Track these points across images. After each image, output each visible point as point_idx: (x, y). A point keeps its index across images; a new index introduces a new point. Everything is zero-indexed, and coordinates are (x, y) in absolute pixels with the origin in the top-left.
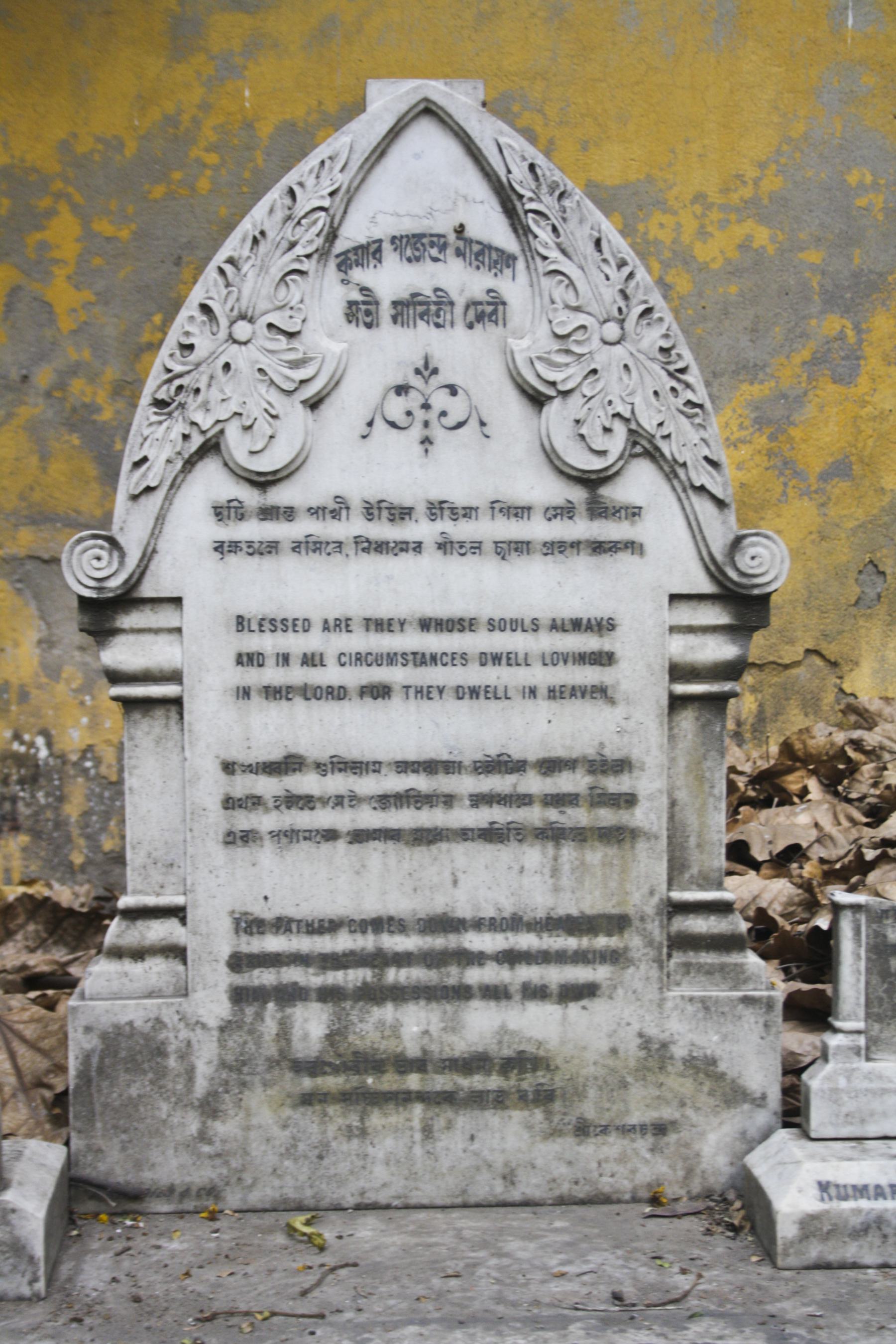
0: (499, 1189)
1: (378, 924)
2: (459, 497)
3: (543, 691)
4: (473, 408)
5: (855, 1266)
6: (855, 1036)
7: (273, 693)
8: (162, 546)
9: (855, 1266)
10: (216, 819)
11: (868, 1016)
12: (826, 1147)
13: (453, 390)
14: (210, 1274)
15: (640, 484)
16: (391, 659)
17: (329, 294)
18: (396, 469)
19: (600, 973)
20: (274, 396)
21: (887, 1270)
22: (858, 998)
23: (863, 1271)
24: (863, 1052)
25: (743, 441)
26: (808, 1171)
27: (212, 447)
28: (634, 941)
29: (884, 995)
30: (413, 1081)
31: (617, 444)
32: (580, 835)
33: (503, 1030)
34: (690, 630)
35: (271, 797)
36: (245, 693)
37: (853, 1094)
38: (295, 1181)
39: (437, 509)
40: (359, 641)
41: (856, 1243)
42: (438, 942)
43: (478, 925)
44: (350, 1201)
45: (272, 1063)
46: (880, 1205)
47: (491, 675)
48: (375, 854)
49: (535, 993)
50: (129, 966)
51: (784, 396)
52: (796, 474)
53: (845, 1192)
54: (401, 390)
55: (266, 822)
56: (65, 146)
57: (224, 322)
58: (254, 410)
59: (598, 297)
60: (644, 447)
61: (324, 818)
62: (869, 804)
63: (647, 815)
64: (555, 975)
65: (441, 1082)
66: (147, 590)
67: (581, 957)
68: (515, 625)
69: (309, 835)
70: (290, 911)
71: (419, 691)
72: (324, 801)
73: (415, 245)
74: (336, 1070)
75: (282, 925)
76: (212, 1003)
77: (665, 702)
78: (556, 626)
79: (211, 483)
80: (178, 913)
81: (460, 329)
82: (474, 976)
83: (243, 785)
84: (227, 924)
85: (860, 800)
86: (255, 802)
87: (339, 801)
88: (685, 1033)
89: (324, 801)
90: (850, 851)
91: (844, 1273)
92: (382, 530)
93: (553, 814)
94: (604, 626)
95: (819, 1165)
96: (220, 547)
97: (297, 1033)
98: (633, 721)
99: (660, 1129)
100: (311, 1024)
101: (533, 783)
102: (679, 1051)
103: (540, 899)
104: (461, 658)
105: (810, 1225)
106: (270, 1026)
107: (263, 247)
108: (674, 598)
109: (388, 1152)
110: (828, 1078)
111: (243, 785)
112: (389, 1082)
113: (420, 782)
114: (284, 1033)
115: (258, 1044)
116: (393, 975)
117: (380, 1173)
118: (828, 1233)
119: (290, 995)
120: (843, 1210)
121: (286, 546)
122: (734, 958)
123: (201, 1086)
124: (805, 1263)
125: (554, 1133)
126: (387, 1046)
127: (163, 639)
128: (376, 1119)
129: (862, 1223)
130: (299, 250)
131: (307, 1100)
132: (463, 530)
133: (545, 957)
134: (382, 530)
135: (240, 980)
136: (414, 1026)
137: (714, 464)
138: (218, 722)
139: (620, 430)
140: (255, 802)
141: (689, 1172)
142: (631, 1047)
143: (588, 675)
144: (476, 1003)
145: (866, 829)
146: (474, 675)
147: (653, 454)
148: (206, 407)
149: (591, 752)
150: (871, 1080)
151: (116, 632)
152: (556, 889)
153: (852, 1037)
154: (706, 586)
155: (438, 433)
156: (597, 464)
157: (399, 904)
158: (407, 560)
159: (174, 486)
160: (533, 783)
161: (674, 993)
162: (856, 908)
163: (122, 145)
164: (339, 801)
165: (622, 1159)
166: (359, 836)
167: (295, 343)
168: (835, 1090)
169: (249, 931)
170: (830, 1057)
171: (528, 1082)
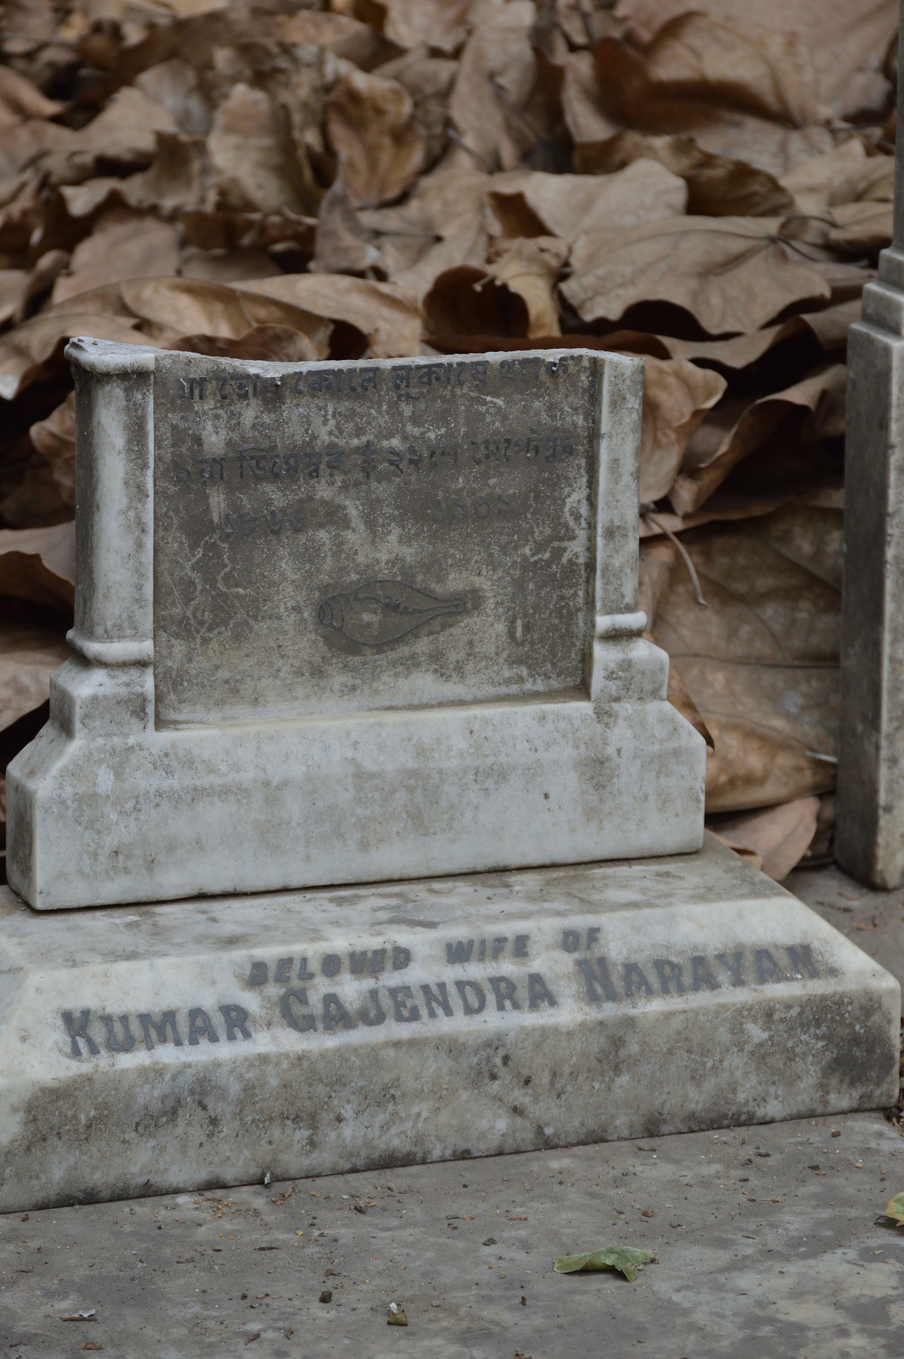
5: (148, 1191)
6: (134, 673)
9: (148, 1191)
11: (159, 624)
12: (70, 929)
21: (219, 1193)
22: (139, 588)
23: (167, 1200)
24: (150, 709)
26: (38, 990)
29: (197, 577)
37: (130, 805)
41: (152, 1142)
46: (201, 1054)
53: (123, 1032)
62: (51, 65)
85: (30, 56)
90: (22, 187)
91: (124, 1207)
95: (63, 974)
110: (73, 772)
118: (89, 1126)
120: (123, 1072)
124: (39, 1196)
129: (164, 1098)
145: (54, 131)
150: (169, 772)
153: (123, 677)
162: (134, 377)
168: (90, 799)
170: (77, 725)
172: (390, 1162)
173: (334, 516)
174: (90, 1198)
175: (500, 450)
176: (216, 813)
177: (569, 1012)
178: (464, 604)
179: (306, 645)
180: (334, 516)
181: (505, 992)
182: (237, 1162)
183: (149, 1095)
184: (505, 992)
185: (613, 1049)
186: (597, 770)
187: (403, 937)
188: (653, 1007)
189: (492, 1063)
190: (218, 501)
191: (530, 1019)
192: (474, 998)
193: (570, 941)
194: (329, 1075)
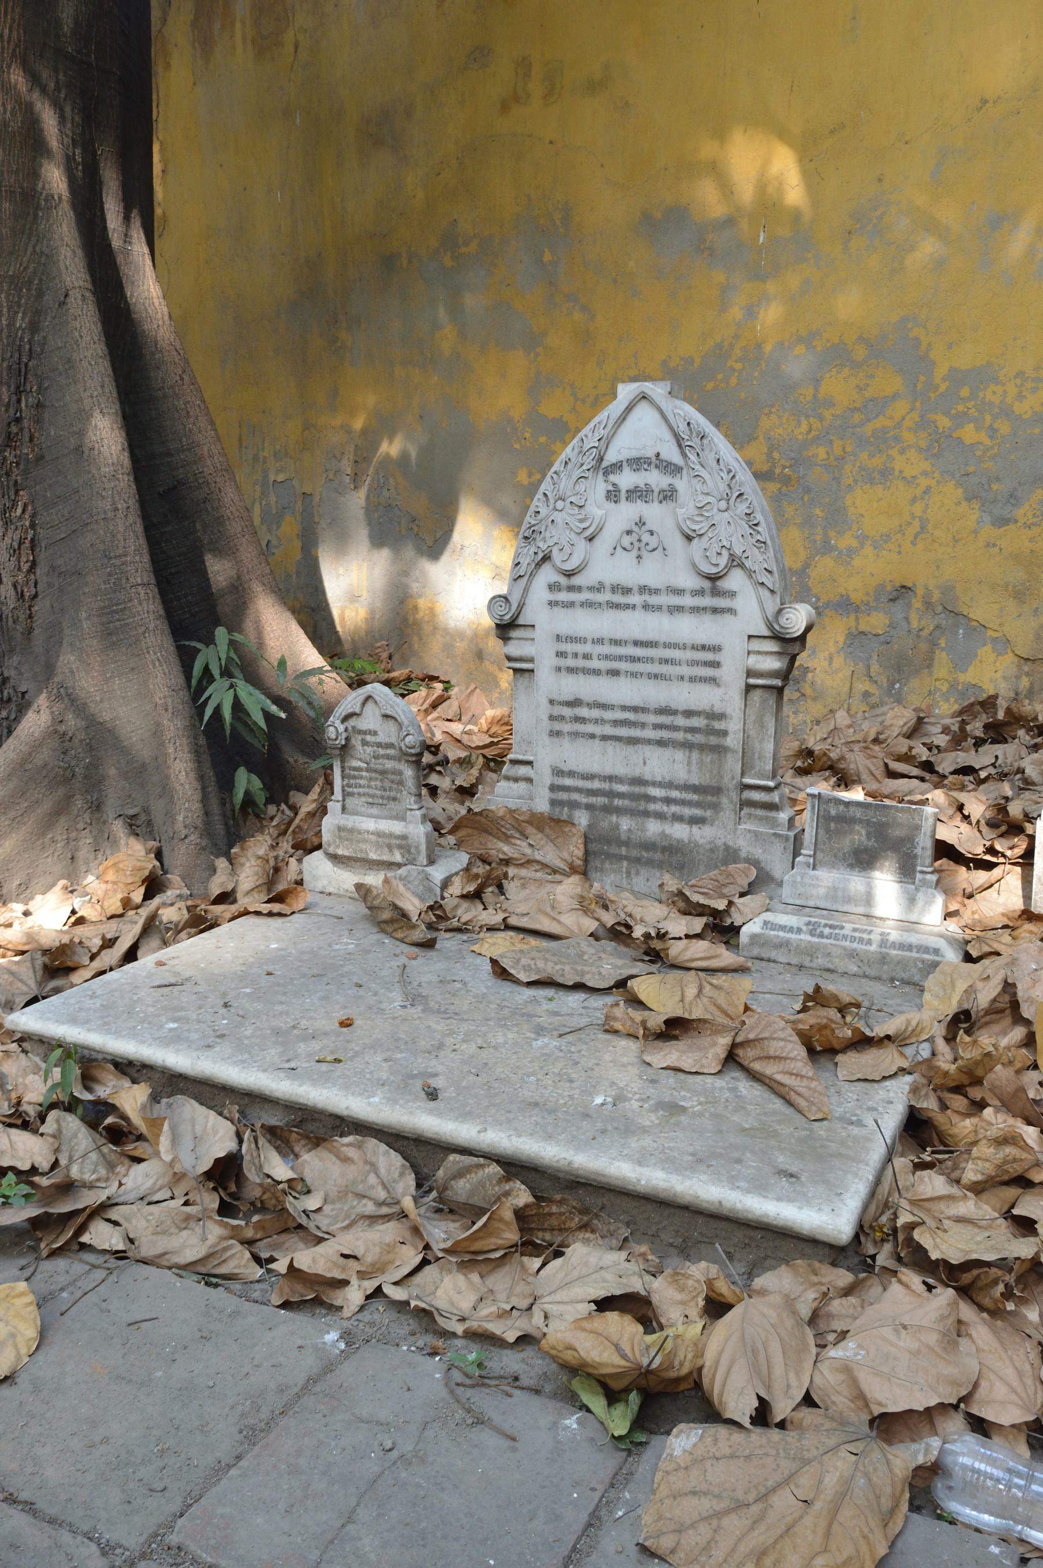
1: (611, 778)
2: (653, 584)
3: (687, 678)
4: (660, 542)
7: (571, 670)
9: (774, 961)
10: (546, 725)
13: (652, 533)
15: (735, 581)
16: (620, 658)
17: (601, 487)
18: (622, 569)
19: (708, 813)
20: (573, 535)
27: (546, 558)
30: (623, 851)
31: (723, 561)
33: (663, 832)
34: (759, 653)
35: (569, 717)
36: (559, 669)
39: (643, 589)
40: (606, 649)
42: (637, 790)
43: (654, 784)
47: (664, 669)
48: (610, 746)
49: (678, 818)
50: (512, 784)
54: (629, 532)
55: (567, 728)
57: (552, 501)
59: (718, 490)
60: (735, 562)
61: (590, 728)
63: (732, 741)
64: (687, 811)
65: (634, 853)
66: (521, 621)
67: (698, 805)
68: (675, 646)
70: (574, 768)
71: (632, 674)
73: (638, 463)
75: (571, 774)
78: (694, 647)
79: (547, 575)
80: (529, 763)
81: (656, 504)
82: (652, 807)
83: (558, 710)
84: (549, 771)
87: (596, 721)
88: (744, 845)
89: (590, 721)
93: (689, 736)
94: (716, 649)
96: (552, 604)
98: (726, 697)
101: (680, 721)
102: (743, 854)
104: (650, 660)
105: (754, 938)
107: (570, 466)
108: (750, 637)
111: (558, 710)
113: (630, 716)
116: (617, 802)
121: (578, 604)
122: (773, 814)
130: (585, 467)
132: (654, 600)
133: (683, 803)
135: (554, 796)
138: (549, 682)
139: (725, 553)
140: (562, 718)
146: (656, 668)
147: (742, 566)
148: (544, 540)
149: (707, 708)
151: (509, 639)
152: (689, 772)
154: (766, 633)
155: (645, 554)
156: (714, 570)
157: (620, 770)
158: (629, 612)
159: (532, 575)
160: (680, 721)
161: (742, 827)
164: (596, 721)
166: (604, 738)
167: (582, 511)
168: (794, 882)
169: (558, 775)
174: (762, 959)
182: (795, 961)
190: (833, 825)
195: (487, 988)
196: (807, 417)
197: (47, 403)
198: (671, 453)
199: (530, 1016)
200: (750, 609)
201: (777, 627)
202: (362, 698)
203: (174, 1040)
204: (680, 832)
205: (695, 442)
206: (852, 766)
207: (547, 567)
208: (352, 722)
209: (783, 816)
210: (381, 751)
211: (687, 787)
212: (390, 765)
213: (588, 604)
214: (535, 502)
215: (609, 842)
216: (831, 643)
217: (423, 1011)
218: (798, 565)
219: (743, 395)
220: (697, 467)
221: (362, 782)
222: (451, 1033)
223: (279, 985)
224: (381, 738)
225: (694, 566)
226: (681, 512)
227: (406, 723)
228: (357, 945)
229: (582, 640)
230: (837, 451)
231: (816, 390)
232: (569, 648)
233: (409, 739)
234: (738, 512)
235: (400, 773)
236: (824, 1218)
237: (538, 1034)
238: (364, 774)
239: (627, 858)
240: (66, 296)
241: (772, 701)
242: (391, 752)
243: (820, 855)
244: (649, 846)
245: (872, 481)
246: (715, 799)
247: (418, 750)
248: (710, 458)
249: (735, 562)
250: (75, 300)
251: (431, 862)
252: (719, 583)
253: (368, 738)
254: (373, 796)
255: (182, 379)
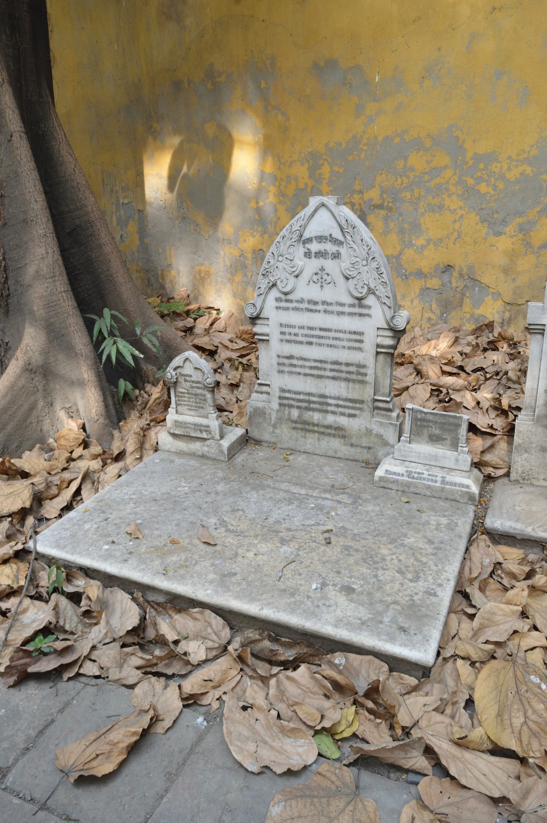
0: (333, 454)
1: (309, 394)
2: (329, 300)
3: (346, 347)
4: (332, 279)
7: (288, 341)
8: (265, 306)
13: (328, 275)
14: (261, 463)
15: (371, 300)
16: (313, 336)
17: (301, 250)
18: (313, 292)
19: (357, 412)
20: (287, 275)
25: (515, 236)
28: (365, 406)
30: (316, 428)
31: (365, 291)
32: (354, 381)
33: (335, 421)
34: (383, 336)
35: (287, 364)
36: (282, 340)
38: (291, 444)
39: (324, 303)
40: (306, 332)
42: (322, 400)
43: (330, 398)
44: (302, 450)
45: (287, 420)
47: (335, 342)
48: (309, 379)
49: (343, 414)
51: (530, 222)
52: (531, 247)
54: (316, 274)
55: (286, 369)
56: (326, 145)
57: (276, 257)
58: (283, 278)
60: (371, 291)
61: (298, 370)
63: (370, 378)
64: (347, 411)
65: (322, 430)
66: (262, 316)
67: (353, 408)
68: (341, 331)
69: (295, 373)
70: (291, 389)
72: (298, 366)
73: (320, 239)
74: (300, 423)
75: (289, 391)
76: (275, 405)
77: (375, 353)
78: (350, 333)
80: (268, 385)
81: (330, 260)
82: (329, 408)
84: (278, 390)
86: (284, 364)
87: (301, 367)
88: (376, 429)
89: (298, 366)
92: (311, 307)
93: (348, 376)
94: (361, 334)
96: (277, 308)
97: (292, 414)
98: (367, 356)
99: (369, 448)
100: (295, 413)
101: (344, 368)
102: (374, 432)
103: (344, 393)
106: (287, 412)
107: (285, 239)
108: (378, 328)
109: (310, 442)
112: (311, 428)
114: (289, 414)
115: (284, 415)
116: (312, 405)
117: (309, 446)
119: (291, 406)
122: (389, 413)
123: (273, 422)
125: (346, 445)
126: (310, 420)
127: (266, 326)
128: (308, 435)
131: (294, 428)
132: (329, 308)
133: (345, 407)
134: (311, 307)
135: (281, 402)
136: (316, 417)
137: (388, 297)
139: (366, 287)
140: (284, 364)
141: (375, 459)
142: (363, 429)
143: (357, 345)
144: (329, 414)
146: (331, 342)
147: (374, 293)
148: (273, 276)
149: (357, 362)
151: (256, 324)
152: (348, 392)
154: (386, 327)
155: (324, 285)
156: (360, 295)
157: (313, 390)
158: (317, 314)
159: (267, 293)
160: (344, 368)
163: (341, 144)
164: (301, 367)
165: (360, 453)
166: (305, 375)
171: (341, 433)
172: (417, 494)
173: (431, 427)
175: (451, 424)
176: (413, 454)
177: (438, 485)
178: (445, 439)
179: (427, 439)
180: (431, 427)
181: (432, 480)
183: (392, 480)
184: (432, 480)
185: (443, 490)
186: (457, 460)
187: (424, 472)
188: (448, 487)
189: (428, 487)
190: (419, 423)
191: (433, 484)
192: (428, 480)
193: (442, 477)
194: (411, 483)
195: (255, 514)
196: (401, 176)
197: (6, 195)
198: (337, 234)
199: (278, 532)
200: (378, 315)
201: (392, 325)
202: (184, 359)
203: (108, 556)
204: (343, 421)
205: (350, 230)
206: (424, 368)
207: (274, 290)
208: (179, 370)
209: (394, 414)
210: (195, 385)
211: (346, 400)
212: (199, 391)
213: (296, 309)
214: (267, 257)
215: (309, 424)
216: (413, 293)
217: (226, 531)
218: (396, 254)
219: (368, 164)
220: (351, 243)
221: (185, 399)
222: (241, 546)
223: (154, 517)
224: (194, 378)
225: (350, 292)
226: (343, 265)
227: (206, 372)
228: (189, 487)
229: (293, 327)
230: (416, 194)
231: (406, 162)
232: (287, 330)
233: (208, 380)
234: (372, 266)
235: (205, 396)
236: (422, 655)
237: (282, 544)
238: (186, 395)
239: (318, 432)
240: (11, 136)
241: (389, 360)
242: (200, 385)
243: (412, 437)
244: (329, 427)
245: (433, 211)
246: (360, 406)
247: (213, 385)
248: (358, 239)
249: (371, 291)
250: (16, 138)
251: (222, 437)
252: (363, 301)
253: (187, 378)
254: (191, 406)
255: (74, 171)
